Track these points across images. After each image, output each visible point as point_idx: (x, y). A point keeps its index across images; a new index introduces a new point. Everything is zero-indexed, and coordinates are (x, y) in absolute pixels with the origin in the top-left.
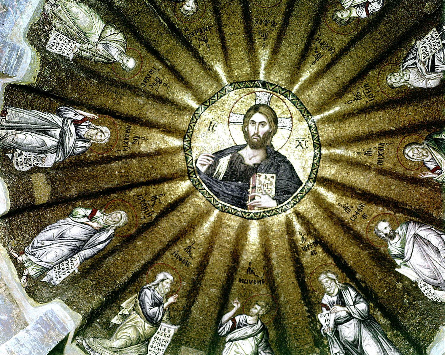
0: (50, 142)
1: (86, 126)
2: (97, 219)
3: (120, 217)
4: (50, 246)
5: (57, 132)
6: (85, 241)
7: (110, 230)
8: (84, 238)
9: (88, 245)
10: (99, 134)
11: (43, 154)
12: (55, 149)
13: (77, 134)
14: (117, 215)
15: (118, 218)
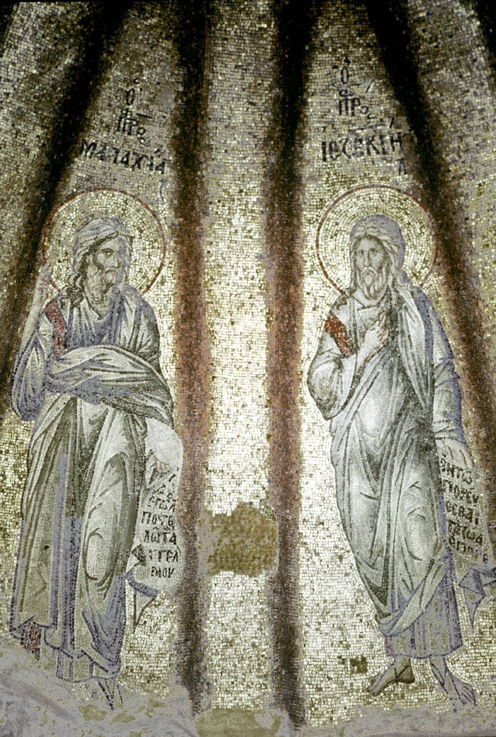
0: (112, 444)
1: (72, 308)
2: (359, 325)
3: (372, 244)
4: (393, 528)
5: (87, 410)
6: (410, 394)
7: (401, 294)
8: (398, 391)
9: (421, 390)
10: (101, 257)
11: (143, 464)
12: (134, 420)
13: (97, 339)
14: (362, 252)
15: (373, 250)
